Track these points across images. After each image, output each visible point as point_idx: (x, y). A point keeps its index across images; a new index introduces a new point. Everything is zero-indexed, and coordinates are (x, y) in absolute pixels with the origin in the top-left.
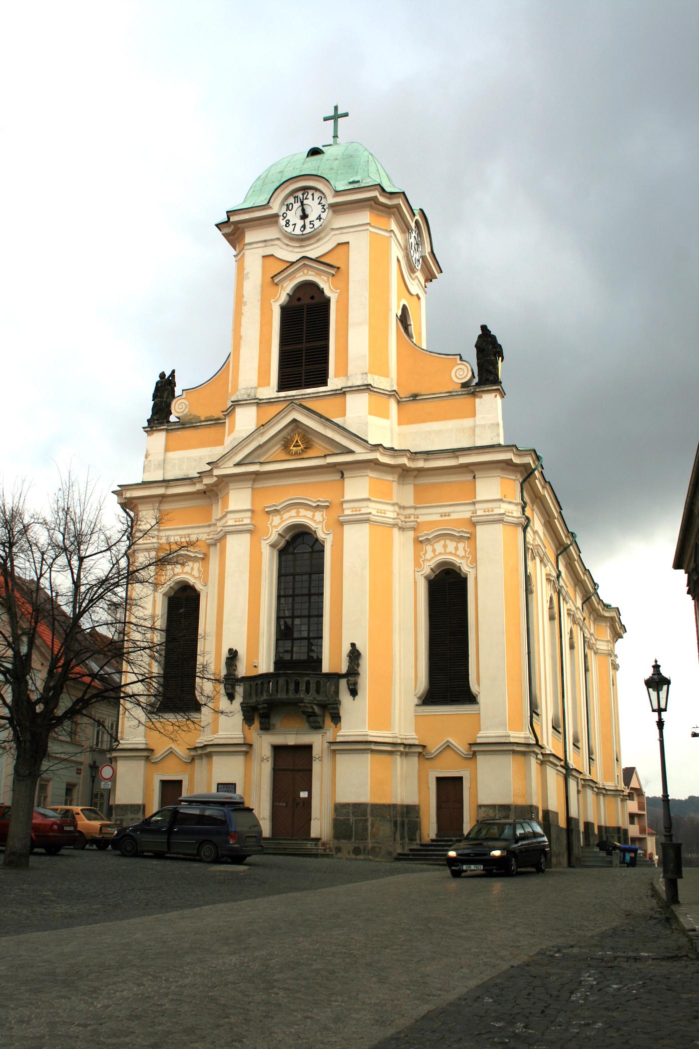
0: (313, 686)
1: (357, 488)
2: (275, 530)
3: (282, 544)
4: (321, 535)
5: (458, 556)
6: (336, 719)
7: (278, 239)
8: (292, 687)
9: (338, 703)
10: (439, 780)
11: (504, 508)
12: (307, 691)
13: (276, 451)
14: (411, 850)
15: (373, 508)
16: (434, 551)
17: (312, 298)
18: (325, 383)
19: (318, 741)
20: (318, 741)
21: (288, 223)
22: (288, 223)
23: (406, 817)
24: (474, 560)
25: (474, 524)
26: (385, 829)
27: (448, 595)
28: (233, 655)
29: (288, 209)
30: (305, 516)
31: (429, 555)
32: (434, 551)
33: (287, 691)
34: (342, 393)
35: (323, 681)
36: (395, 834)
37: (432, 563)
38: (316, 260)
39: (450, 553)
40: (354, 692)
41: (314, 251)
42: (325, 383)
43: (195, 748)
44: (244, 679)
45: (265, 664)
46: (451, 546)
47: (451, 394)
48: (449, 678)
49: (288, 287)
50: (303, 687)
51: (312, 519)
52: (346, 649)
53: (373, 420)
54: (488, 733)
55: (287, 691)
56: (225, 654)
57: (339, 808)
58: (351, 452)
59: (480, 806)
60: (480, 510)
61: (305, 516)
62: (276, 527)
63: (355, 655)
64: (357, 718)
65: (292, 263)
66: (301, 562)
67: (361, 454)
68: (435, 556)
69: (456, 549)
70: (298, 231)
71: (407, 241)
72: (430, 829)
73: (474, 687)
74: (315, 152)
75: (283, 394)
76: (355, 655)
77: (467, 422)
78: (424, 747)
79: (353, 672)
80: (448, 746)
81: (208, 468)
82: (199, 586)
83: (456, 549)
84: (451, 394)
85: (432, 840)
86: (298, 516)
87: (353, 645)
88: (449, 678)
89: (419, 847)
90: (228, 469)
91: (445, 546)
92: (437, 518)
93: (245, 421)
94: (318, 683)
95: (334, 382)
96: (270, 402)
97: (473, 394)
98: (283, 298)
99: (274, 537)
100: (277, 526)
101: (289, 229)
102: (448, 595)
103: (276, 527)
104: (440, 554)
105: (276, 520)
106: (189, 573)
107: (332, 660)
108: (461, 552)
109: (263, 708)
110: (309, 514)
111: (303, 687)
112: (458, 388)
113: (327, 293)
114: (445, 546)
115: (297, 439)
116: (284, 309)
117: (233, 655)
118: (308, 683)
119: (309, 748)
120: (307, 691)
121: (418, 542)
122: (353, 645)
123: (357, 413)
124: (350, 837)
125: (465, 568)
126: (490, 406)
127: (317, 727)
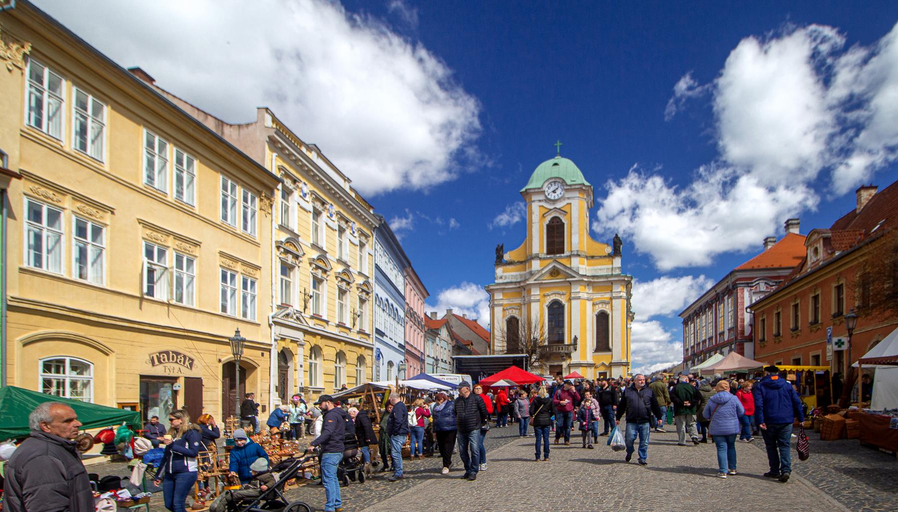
1: (576, 289)
6: (570, 357)
13: (547, 276)
15: (581, 295)
18: (563, 252)
19: (565, 364)
20: (565, 364)
27: (603, 320)
34: (570, 257)
42: (563, 252)
47: (605, 257)
48: (603, 344)
52: (573, 337)
54: (615, 360)
64: (576, 358)
66: (556, 311)
74: (556, 164)
88: (603, 344)
90: (531, 281)
93: (536, 265)
95: (567, 253)
98: (547, 222)
102: (603, 320)
115: (555, 272)
121: (594, 305)
123: (575, 263)
125: (609, 312)
127: (564, 360)
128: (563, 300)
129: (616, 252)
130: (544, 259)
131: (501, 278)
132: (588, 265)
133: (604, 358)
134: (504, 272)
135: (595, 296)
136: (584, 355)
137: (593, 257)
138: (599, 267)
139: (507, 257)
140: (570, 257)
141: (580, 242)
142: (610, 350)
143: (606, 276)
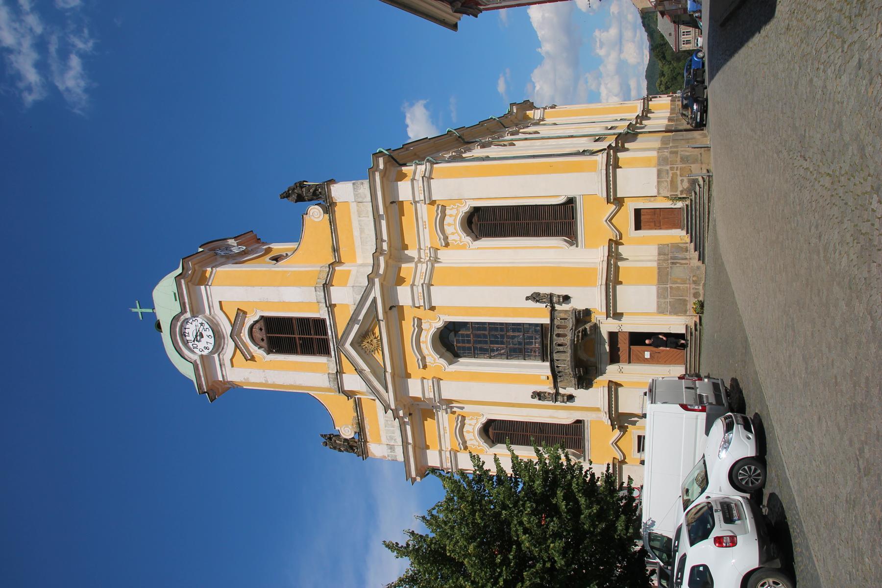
0: (560, 331)
2: (437, 361)
3: (449, 355)
4: (440, 324)
5: (457, 215)
6: (587, 312)
7: (219, 355)
8: (561, 349)
9: (575, 310)
10: (638, 227)
11: (418, 177)
12: (565, 336)
14: (695, 250)
16: (453, 234)
17: (261, 329)
18: (324, 321)
21: (206, 348)
22: (206, 348)
23: (669, 256)
24: (459, 200)
25: (433, 203)
26: (678, 272)
28: (539, 395)
29: (196, 348)
30: (426, 337)
31: (456, 237)
32: (453, 234)
33: (564, 352)
34: (331, 307)
35: (556, 322)
36: (681, 264)
37: (463, 235)
38: (233, 326)
39: (455, 220)
40: (566, 299)
41: (226, 328)
42: (324, 321)
43: (612, 425)
44: (556, 386)
45: (542, 369)
46: (447, 220)
47: (332, 222)
49: (253, 348)
50: (561, 340)
51: (428, 331)
52: (531, 304)
53: (351, 282)
55: (564, 352)
56: (536, 401)
57: (661, 311)
58: (374, 300)
59: (658, 193)
60: (420, 196)
61: (426, 337)
62: (435, 360)
63: (536, 297)
64: (588, 297)
65: (237, 346)
67: (376, 292)
68: (457, 232)
69: (451, 216)
70: (212, 341)
71: (222, 256)
72: (678, 235)
73: (561, 200)
75: (333, 353)
76: (536, 297)
77: (353, 207)
78: (610, 240)
79: (550, 299)
80: (610, 220)
81: (390, 411)
82: (484, 420)
83: (451, 216)
84: (332, 222)
85: (687, 233)
86: (426, 342)
87: (527, 298)
89: (693, 244)
90: (390, 397)
91: (449, 225)
92: (427, 231)
93: (352, 381)
94: (558, 327)
95: (323, 314)
96: (339, 363)
97: (333, 204)
99: (442, 362)
100: (434, 359)
101: (211, 347)
103: (435, 360)
104: (455, 229)
105: (428, 360)
106: (473, 428)
107: (540, 316)
108: (454, 212)
109: (579, 371)
110: (424, 334)
111: (561, 340)
112: (327, 216)
113: (257, 318)
114: (449, 225)
116: (269, 352)
117: (539, 395)
118: (558, 335)
119: (613, 336)
120: (565, 336)
122: (527, 298)
123: (345, 296)
124: (685, 300)
125: (465, 208)
126: (340, 191)
127: (596, 328)
128: (433, 325)
129: (319, 195)
130: (339, 363)
131: (392, 448)
132: (353, 257)
133: (592, 219)
134: (379, 442)
135: (426, 242)
136: (581, 276)
137: (336, 250)
138: (356, 233)
139: (347, 432)
140: (331, 307)
141: (297, 280)
142: (571, 201)
143: (377, 218)
